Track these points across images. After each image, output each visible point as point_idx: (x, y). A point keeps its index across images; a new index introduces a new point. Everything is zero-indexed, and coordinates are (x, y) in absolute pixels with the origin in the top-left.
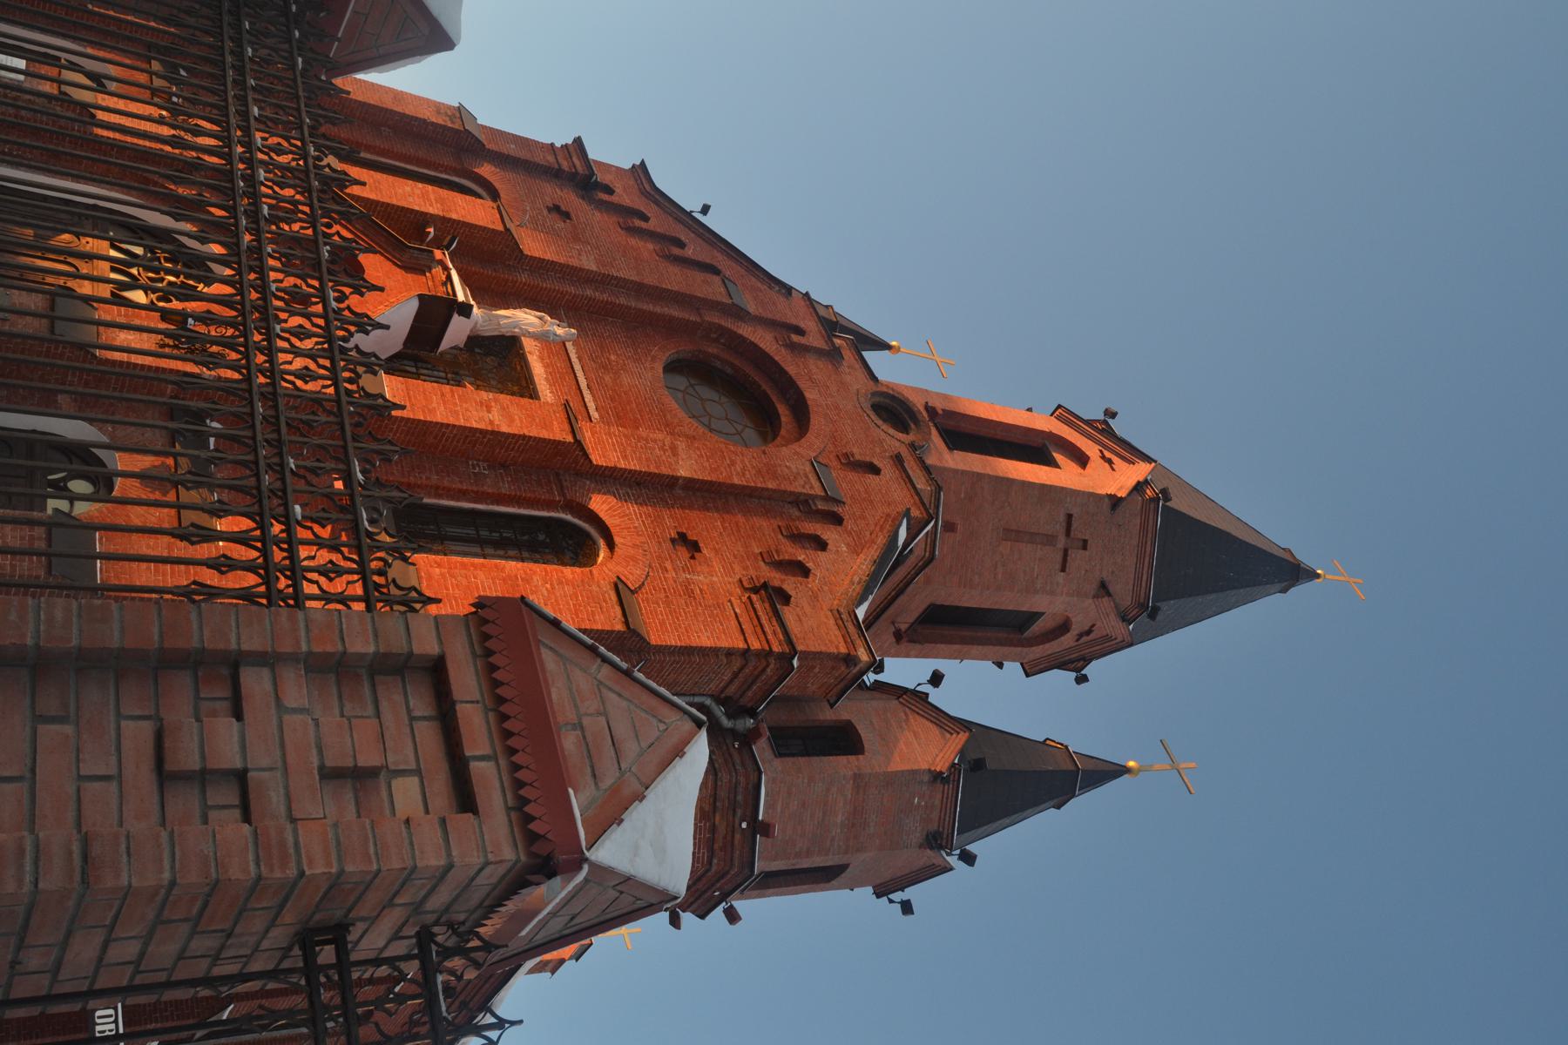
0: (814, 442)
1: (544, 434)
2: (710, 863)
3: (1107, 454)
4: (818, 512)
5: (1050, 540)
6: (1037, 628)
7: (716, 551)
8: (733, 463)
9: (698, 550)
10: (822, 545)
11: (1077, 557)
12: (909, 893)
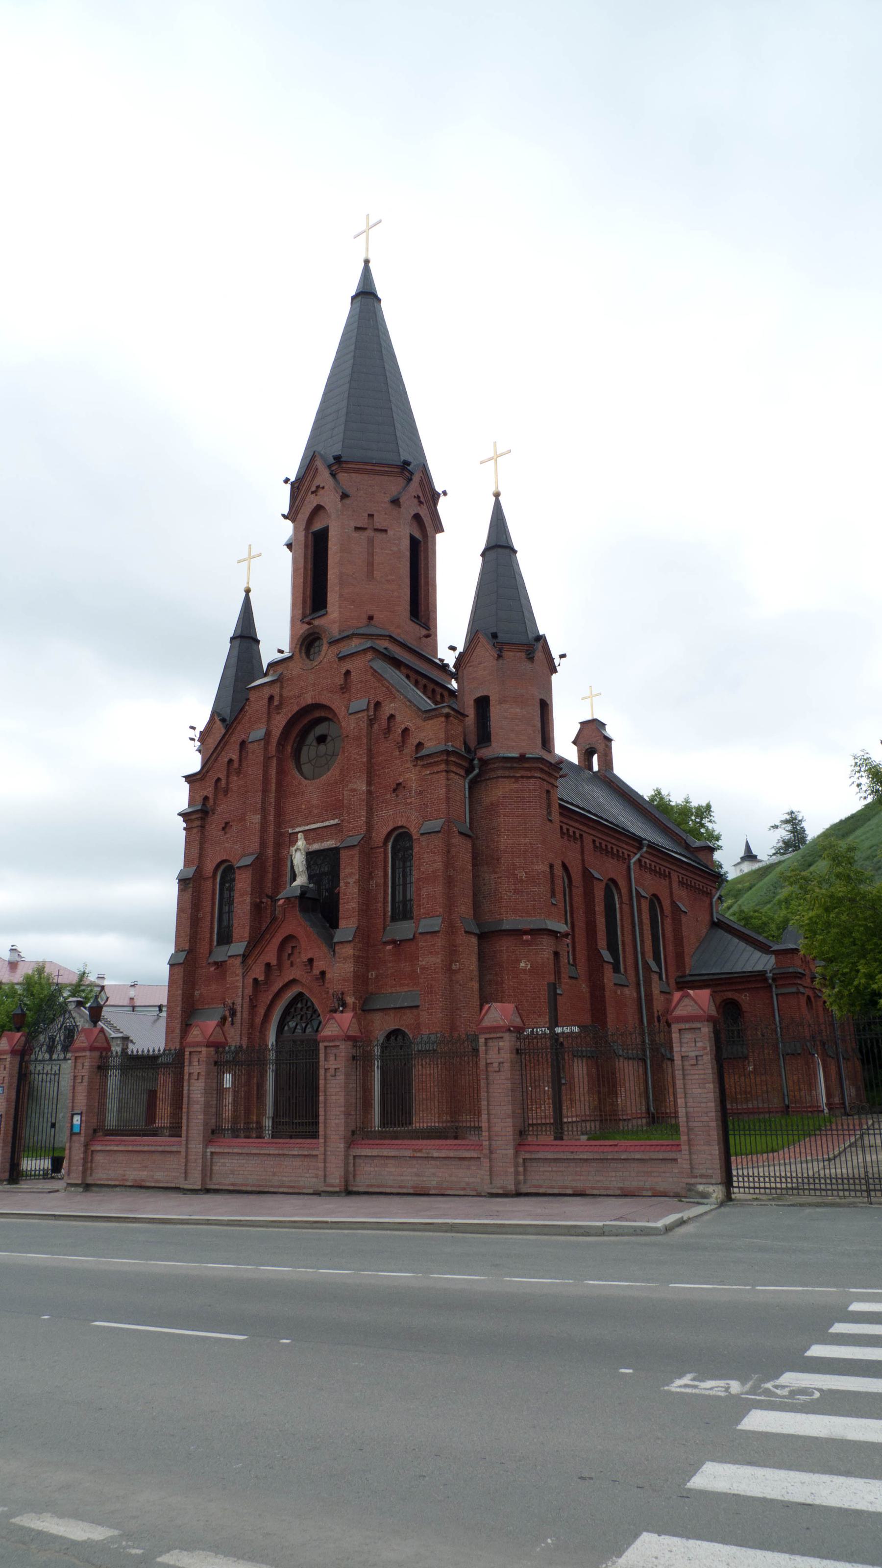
0: (336, 703)
1: (357, 858)
2: (536, 777)
3: (313, 489)
4: (375, 714)
5: (371, 541)
6: (418, 535)
7: (400, 775)
8: (355, 759)
9: (400, 784)
10: (392, 717)
11: (379, 522)
12: (555, 654)
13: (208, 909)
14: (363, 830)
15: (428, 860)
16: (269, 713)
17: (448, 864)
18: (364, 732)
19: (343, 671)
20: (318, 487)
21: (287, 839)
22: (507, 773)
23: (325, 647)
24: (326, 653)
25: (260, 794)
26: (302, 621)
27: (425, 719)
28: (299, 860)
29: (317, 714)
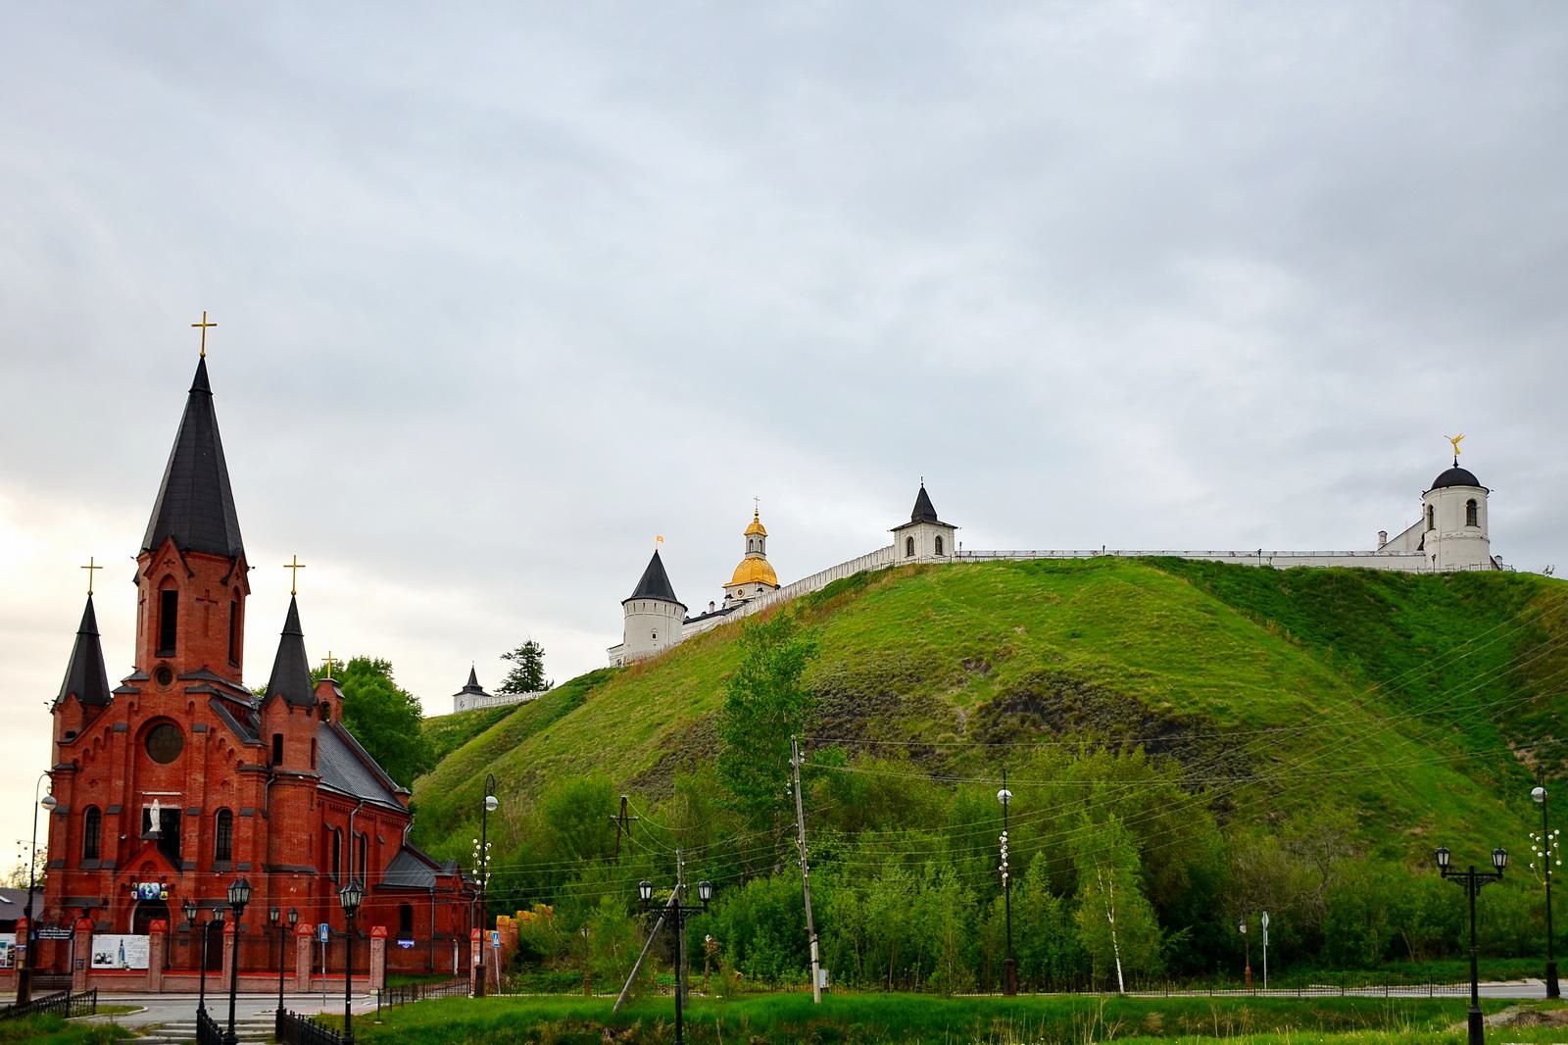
1: (197, 823)
3: (166, 560)
5: (207, 609)
13: (78, 834)
14: (201, 805)
15: (244, 829)
16: (130, 714)
17: (255, 833)
18: (204, 745)
19: (189, 702)
20: (169, 560)
21: (141, 798)
22: (291, 783)
23: (174, 681)
24: (176, 686)
25: (123, 768)
26: (157, 654)
27: (247, 747)
28: (155, 816)
29: (165, 722)
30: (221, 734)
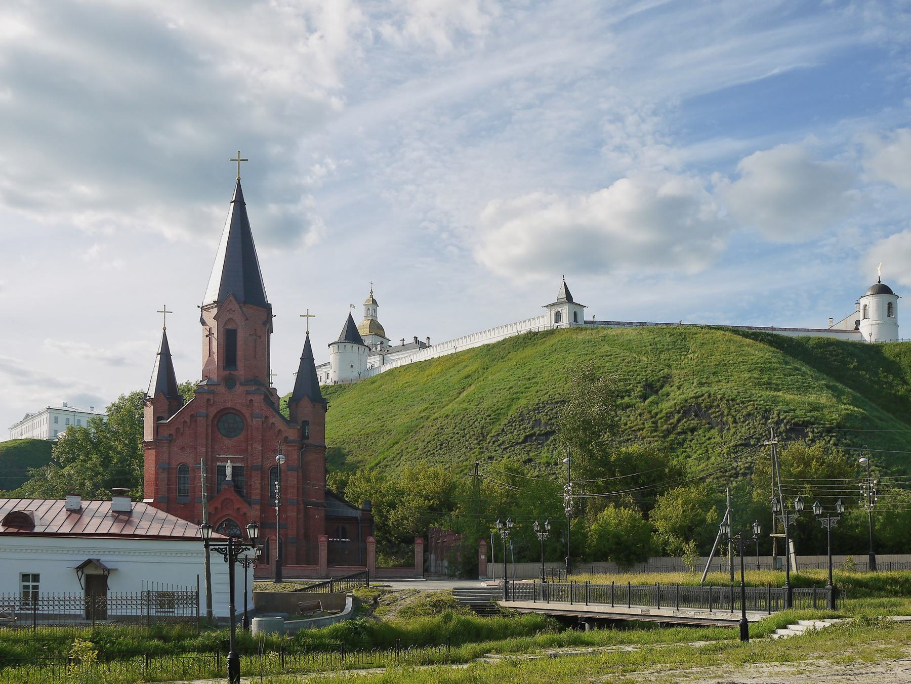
23: (238, 385)
24: (239, 389)
26: (225, 369)
28: (229, 471)
29: (231, 411)
30: (272, 420)
